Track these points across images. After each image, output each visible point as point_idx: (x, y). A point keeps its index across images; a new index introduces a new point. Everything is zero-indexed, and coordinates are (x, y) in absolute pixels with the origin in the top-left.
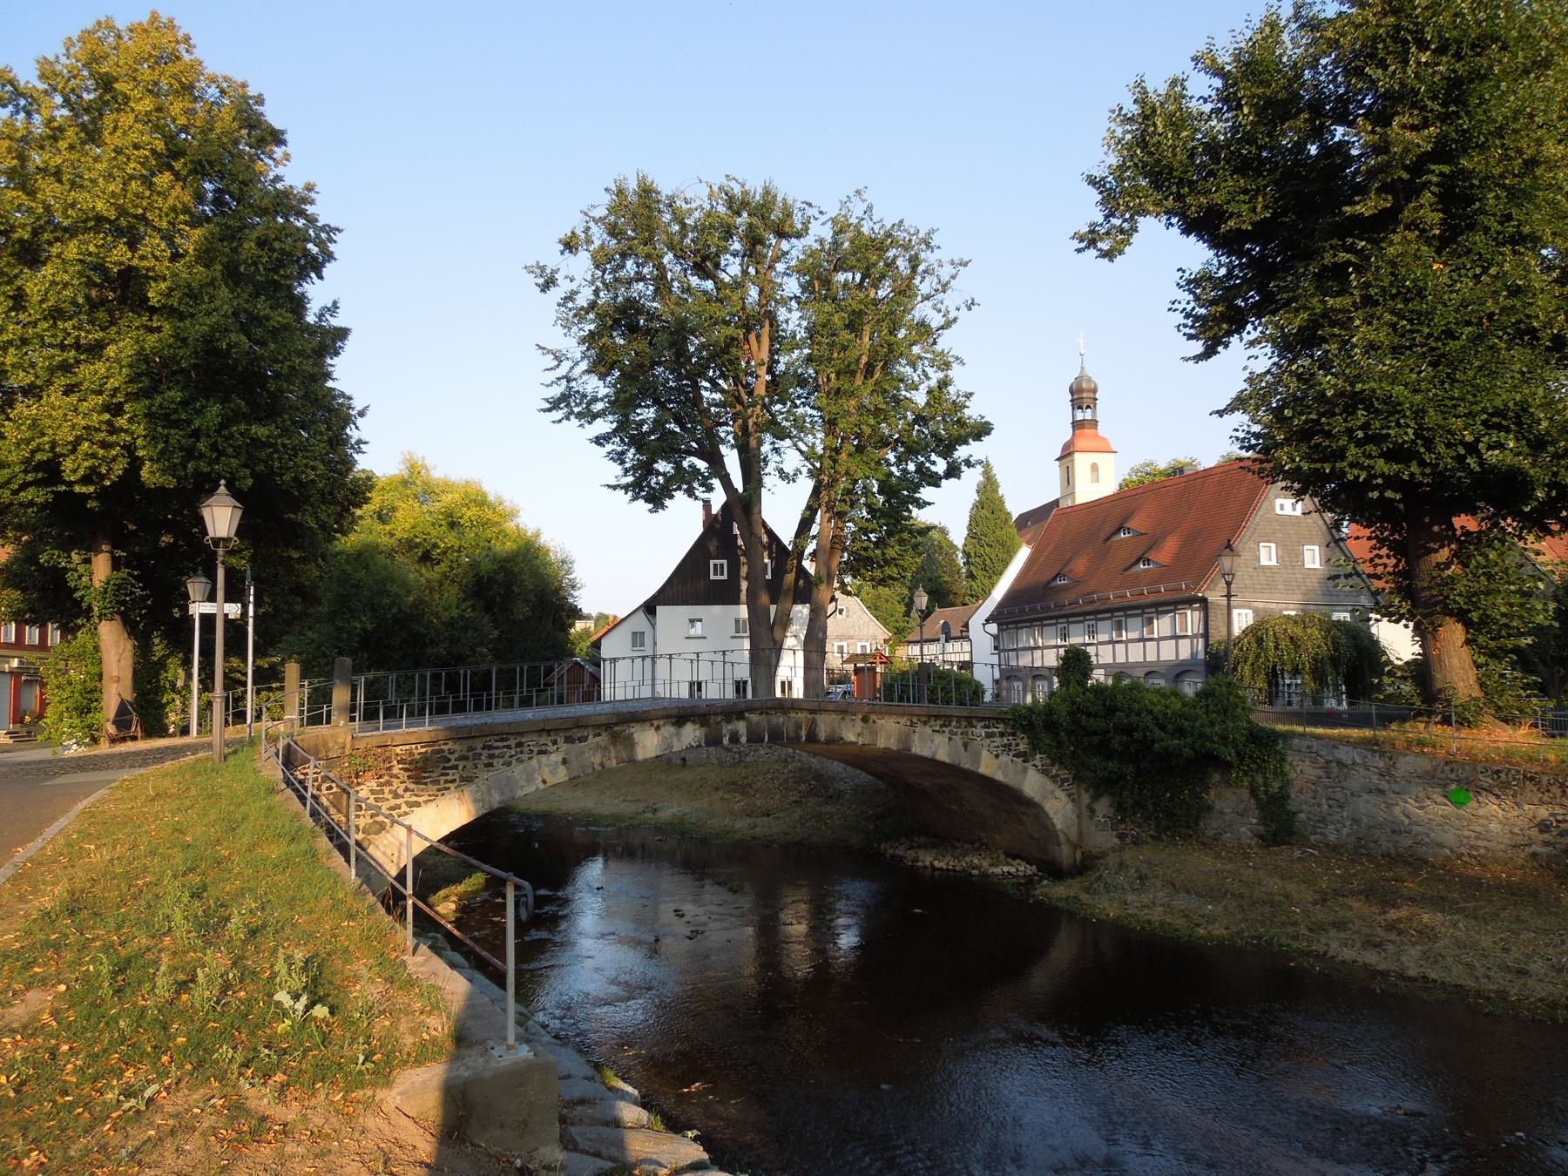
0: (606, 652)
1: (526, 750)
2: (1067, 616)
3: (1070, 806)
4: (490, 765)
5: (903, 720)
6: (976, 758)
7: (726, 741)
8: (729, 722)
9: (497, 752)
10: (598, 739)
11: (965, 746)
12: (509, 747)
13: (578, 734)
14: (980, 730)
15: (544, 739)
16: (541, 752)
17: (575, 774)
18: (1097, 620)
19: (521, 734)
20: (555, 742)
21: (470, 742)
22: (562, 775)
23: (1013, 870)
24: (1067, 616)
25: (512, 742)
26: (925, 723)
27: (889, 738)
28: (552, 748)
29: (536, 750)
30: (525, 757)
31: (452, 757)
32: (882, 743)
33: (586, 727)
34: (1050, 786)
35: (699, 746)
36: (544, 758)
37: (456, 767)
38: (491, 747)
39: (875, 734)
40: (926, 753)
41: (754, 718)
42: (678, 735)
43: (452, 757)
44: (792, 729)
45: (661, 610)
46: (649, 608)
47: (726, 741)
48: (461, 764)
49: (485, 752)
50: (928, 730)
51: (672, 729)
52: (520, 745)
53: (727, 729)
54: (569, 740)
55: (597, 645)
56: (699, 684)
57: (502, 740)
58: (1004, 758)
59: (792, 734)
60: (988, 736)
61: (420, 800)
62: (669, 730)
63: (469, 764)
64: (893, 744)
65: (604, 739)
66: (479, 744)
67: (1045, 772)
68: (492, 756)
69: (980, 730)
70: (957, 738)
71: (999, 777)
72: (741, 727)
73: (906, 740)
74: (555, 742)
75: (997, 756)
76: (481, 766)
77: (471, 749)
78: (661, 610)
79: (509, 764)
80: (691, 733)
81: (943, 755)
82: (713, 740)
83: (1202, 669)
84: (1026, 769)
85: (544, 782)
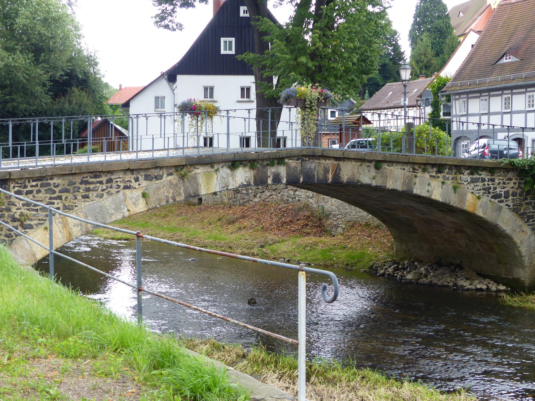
0: (133, 109)
1: (114, 185)
2: (512, 88)
4: (87, 197)
5: (407, 168)
6: (463, 199)
7: (270, 181)
8: (272, 165)
9: (92, 186)
10: (170, 178)
11: (455, 188)
12: (101, 183)
13: (156, 172)
14: (466, 177)
15: (129, 177)
16: (126, 188)
17: (152, 205)
19: (111, 172)
20: (137, 180)
21: (71, 178)
22: (141, 207)
23: (484, 287)
24: (512, 88)
25: (104, 179)
26: (424, 171)
27: (396, 182)
28: (134, 184)
29: (122, 185)
30: (113, 190)
31: (57, 190)
32: (390, 185)
33: (161, 168)
34: (520, 222)
35: (249, 184)
36: (127, 191)
37: (60, 198)
38: (87, 183)
39: (385, 177)
40: (424, 194)
41: (293, 163)
42: (233, 176)
43: (57, 190)
44: (321, 172)
45: (179, 77)
46: (171, 76)
47: (270, 181)
48: (64, 195)
49: (83, 186)
50: (427, 175)
51: (228, 171)
52: (110, 181)
53: (271, 171)
54: (147, 178)
55: (127, 105)
56: (211, 139)
57: (96, 177)
58: (485, 199)
59: (321, 177)
60: (473, 181)
61: (32, 223)
62: (225, 171)
63: (70, 196)
64: (399, 187)
65: (174, 178)
66: (77, 179)
67: (515, 210)
68: (88, 190)
70: (449, 182)
71: (480, 213)
72: (282, 170)
73: (409, 182)
74: (137, 180)
75: (479, 198)
77: (71, 184)
78: (179, 77)
79: (101, 196)
80: (242, 175)
81: (437, 195)
84: (500, 208)
85: (129, 210)
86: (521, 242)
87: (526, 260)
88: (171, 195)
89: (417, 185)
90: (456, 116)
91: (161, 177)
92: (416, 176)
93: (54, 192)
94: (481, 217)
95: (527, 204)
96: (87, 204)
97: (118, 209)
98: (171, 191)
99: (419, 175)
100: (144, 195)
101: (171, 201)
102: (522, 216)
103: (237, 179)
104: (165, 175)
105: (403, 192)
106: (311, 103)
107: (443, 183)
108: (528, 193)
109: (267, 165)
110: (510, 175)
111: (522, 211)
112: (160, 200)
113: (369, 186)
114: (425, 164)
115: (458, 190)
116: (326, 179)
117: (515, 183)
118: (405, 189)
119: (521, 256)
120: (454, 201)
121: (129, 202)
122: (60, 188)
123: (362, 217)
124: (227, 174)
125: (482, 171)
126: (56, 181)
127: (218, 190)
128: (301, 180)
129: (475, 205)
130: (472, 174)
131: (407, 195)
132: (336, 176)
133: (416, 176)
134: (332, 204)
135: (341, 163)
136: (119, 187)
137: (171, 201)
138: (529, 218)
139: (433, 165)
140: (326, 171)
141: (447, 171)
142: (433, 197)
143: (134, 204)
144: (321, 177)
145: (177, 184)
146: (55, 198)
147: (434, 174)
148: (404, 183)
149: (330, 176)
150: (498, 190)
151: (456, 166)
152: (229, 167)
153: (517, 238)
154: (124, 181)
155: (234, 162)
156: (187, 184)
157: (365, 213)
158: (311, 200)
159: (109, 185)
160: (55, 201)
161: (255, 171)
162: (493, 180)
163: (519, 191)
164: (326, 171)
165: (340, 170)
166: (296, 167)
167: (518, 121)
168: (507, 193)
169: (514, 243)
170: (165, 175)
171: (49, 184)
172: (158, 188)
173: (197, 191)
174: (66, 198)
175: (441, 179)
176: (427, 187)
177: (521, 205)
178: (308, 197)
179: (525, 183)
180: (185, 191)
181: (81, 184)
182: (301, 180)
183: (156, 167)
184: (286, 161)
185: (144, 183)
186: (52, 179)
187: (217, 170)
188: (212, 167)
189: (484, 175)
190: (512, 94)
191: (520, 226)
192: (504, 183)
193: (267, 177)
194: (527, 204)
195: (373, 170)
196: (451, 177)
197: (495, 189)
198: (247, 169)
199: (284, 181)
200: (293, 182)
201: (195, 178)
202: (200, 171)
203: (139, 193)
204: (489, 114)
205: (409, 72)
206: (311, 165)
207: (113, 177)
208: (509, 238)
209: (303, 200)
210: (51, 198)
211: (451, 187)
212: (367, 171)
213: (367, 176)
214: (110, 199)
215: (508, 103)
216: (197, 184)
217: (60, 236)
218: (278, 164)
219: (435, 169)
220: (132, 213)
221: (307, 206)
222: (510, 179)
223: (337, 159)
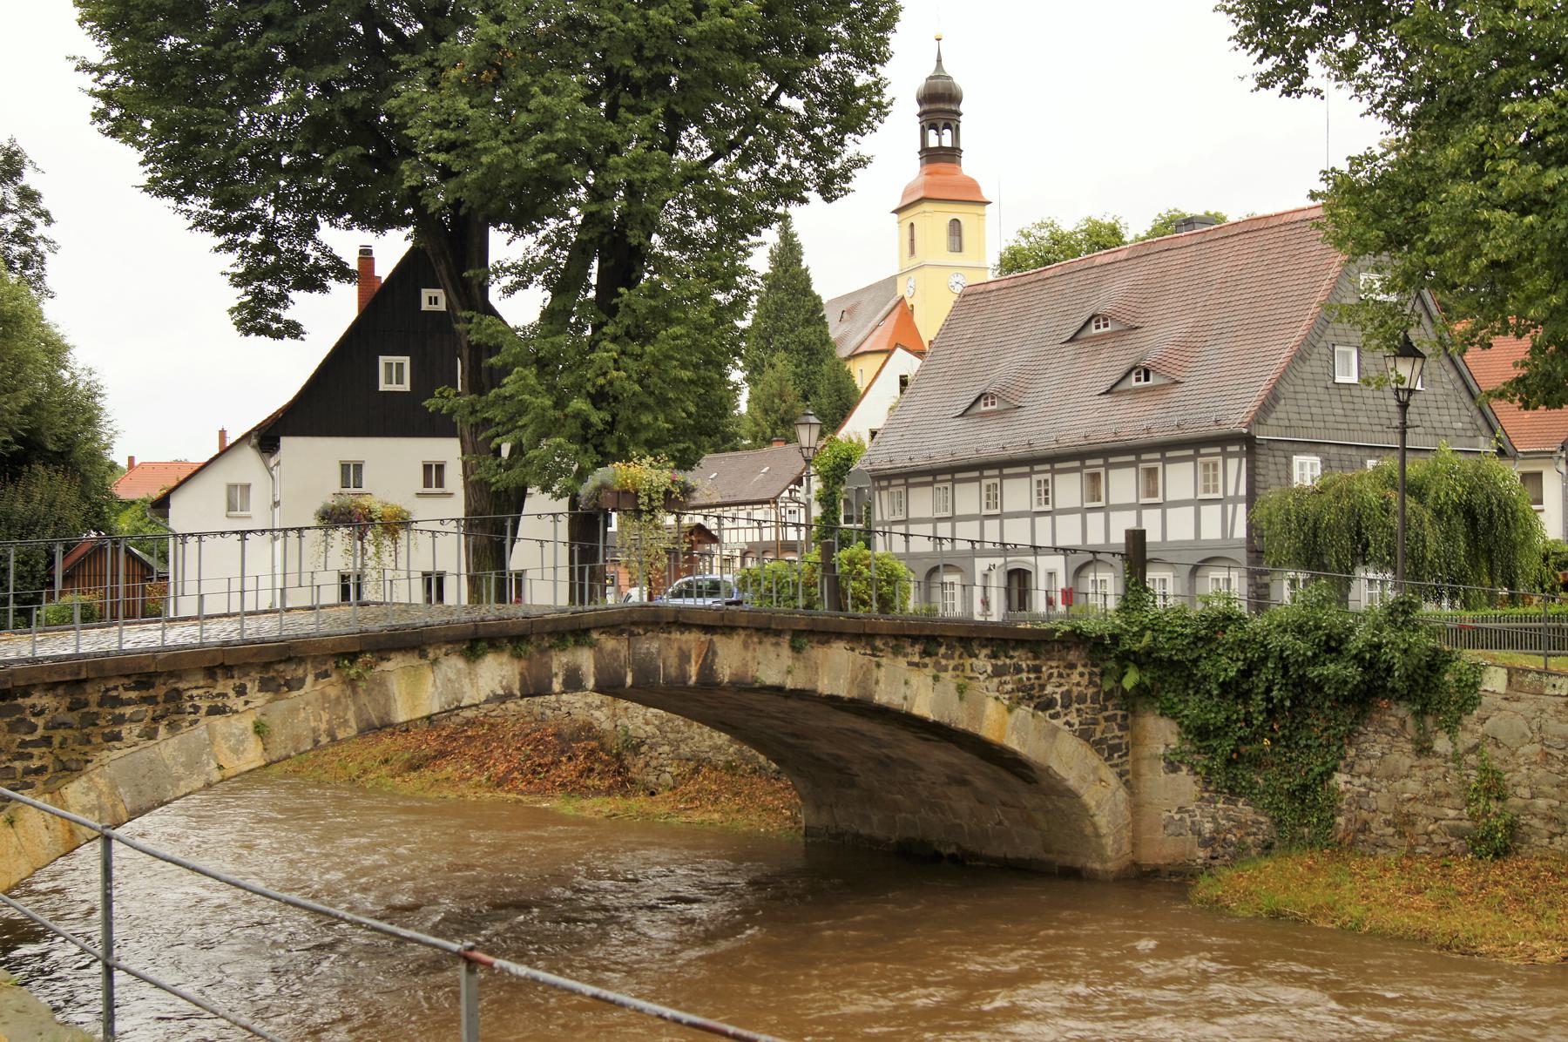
0: (181, 516)
3: (1122, 794)
6: (977, 714)
7: (557, 685)
9: (128, 711)
11: (961, 690)
13: (290, 672)
14: (983, 663)
16: (214, 711)
18: (1054, 472)
20: (241, 691)
22: (253, 755)
25: (160, 691)
26: (897, 651)
27: (837, 678)
28: (236, 702)
29: (204, 705)
32: (825, 686)
33: (301, 660)
34: (1094, 760)
36: (218, 721)
37: (47, 741)
41: (609, 643)
43: (40, 722)
44: (673, 661)
45: (285, 442)
46: (267, 438)
48: (57, 737)
50: (902, 662)
53: (559, 661)
55: (161, 505)
58: (1024, 711)
59: (673, 672)
60: (998, 672)
62: (453, 665)
64: (843, 689)
65: (332, 687)
67: (1085, 735)
68: (120, 720)
69: (983, 663)
70: (947, 676)
71: (1013, 743)
72: (585, 660)
74: (241, 691)
76: (97, 740)
78: (285, 442)
79: (150, 734)
80: (494, 673)
81: (923, 707)
82: (535, 687)
83: (1242, 555)
84: (1056, 730)
85: (220, 767)
86: (1098, 805)
87: (1109, 842)
88: (324, 726)
89: (881, 684)
90: (883, 523)
91: (300, 683)
92: (878, 665)
93: (33, 728)
94: (1015, 753)
95: (1107, 719)
96: (116, 754)
97: (193, 764)
98: (325, 717)
99: (884, 661)
100: (259, 729)
101: (324, 740)
102: (1097, 745)
103: (481, 682)
104: (310, 679)
105: (852, 700)
106: (651, 499)
107: (936, 678)
108: (1109, 695)
109: (551, 647)
110: (1072, 656)
111: (1098, 735)
112: (297, 739)
113: (778, 690)
114: (896, 637)
115: (967, 693)
116: (684, 676)
117: (1082, 675)
118: (855, 694)
119: (1098, 836)
120: (957, 716)
121: (223, 748)
122: (48, 716)
123: (718, 748)
124: (459, 671)
125: (1014, 649)
126: (39, 699)
127: (436, 709)
128: (629, 680)
129: (1002, 726)
130: (994, 656)
131: (862, 708)
132: (707, 669)
133: (878, 665)
134: (640, 719)
135: (716, 638)
136: (197, 709)
137: (324, 740)
138: (1113, 749)
139: (915, 639)
140: (684, 657)
141: (943, 650)
142: (916, 711)
143: (235, 751)
144: (673, 672)
145: (338, 700)
146: (35, 744)
147: (916, 659)
148: (852, 682)
149: (693, 670)
150: (1049, 689)
151: (960, 639)
152: (462, 654)
153: (1090, 796)
154: (208, 696)
155: (474, 642)
156: (364, 699)
157: (721, 738)
158: (597, 714)
159: (171, 706)
160: (36, 751)
161: (524, 663)
162: (1037, 669)
163: (1091, 691)
164: (684, 657)
165: (715, 653)
166: (616, 651)
167: (1017, 532)
168: (1067, 696)
169: (1084, 808)
170: (310, 679)
171: (20, 709)
172: (294, 711)
173: (388, 714)
174: (64, 741)
175: (930, 671)
176: (903, 689)
177: (1095, 722)
178: (590, 705)
179: (1102, 674)
180: (358, 716)
181: (100, 705)
182: (629, 680)
183: (289, 660)
184: (595, 635)
185: (259, 699)
186: (26, 694)
187: (435, 662)
188: (423, 655)
189: (1022, 658)
190: (1002, 477)
191: (1095, 770)
192: (1060, 675)
193: (551, 677)
194: (1107, 719)
195: (786, 651)
196: (952, 664)
197: (1043, 687)
198: (505, 658)
199: (591, 683)
200: (610, 686)
201: (381, 683)
202: (395, 666)
203: (247, 722)
204: (952, 519)
205: (815, 431)
206: (651, 645)
207: (181, 686)
208: (1073, 795)
209: (580, 715)
210: (24, 744)
211: (952, 687)
212: (773, 656)
213: (773, 666)
214: (174, 741)
215: (994, 496)
216: (388, 698)
217: (46, 840)
218: (577, 643)
219: (918, 648)
220: (228, 773)
221: (588, 729)
222: (1072, 666)
223: (708, 629)
